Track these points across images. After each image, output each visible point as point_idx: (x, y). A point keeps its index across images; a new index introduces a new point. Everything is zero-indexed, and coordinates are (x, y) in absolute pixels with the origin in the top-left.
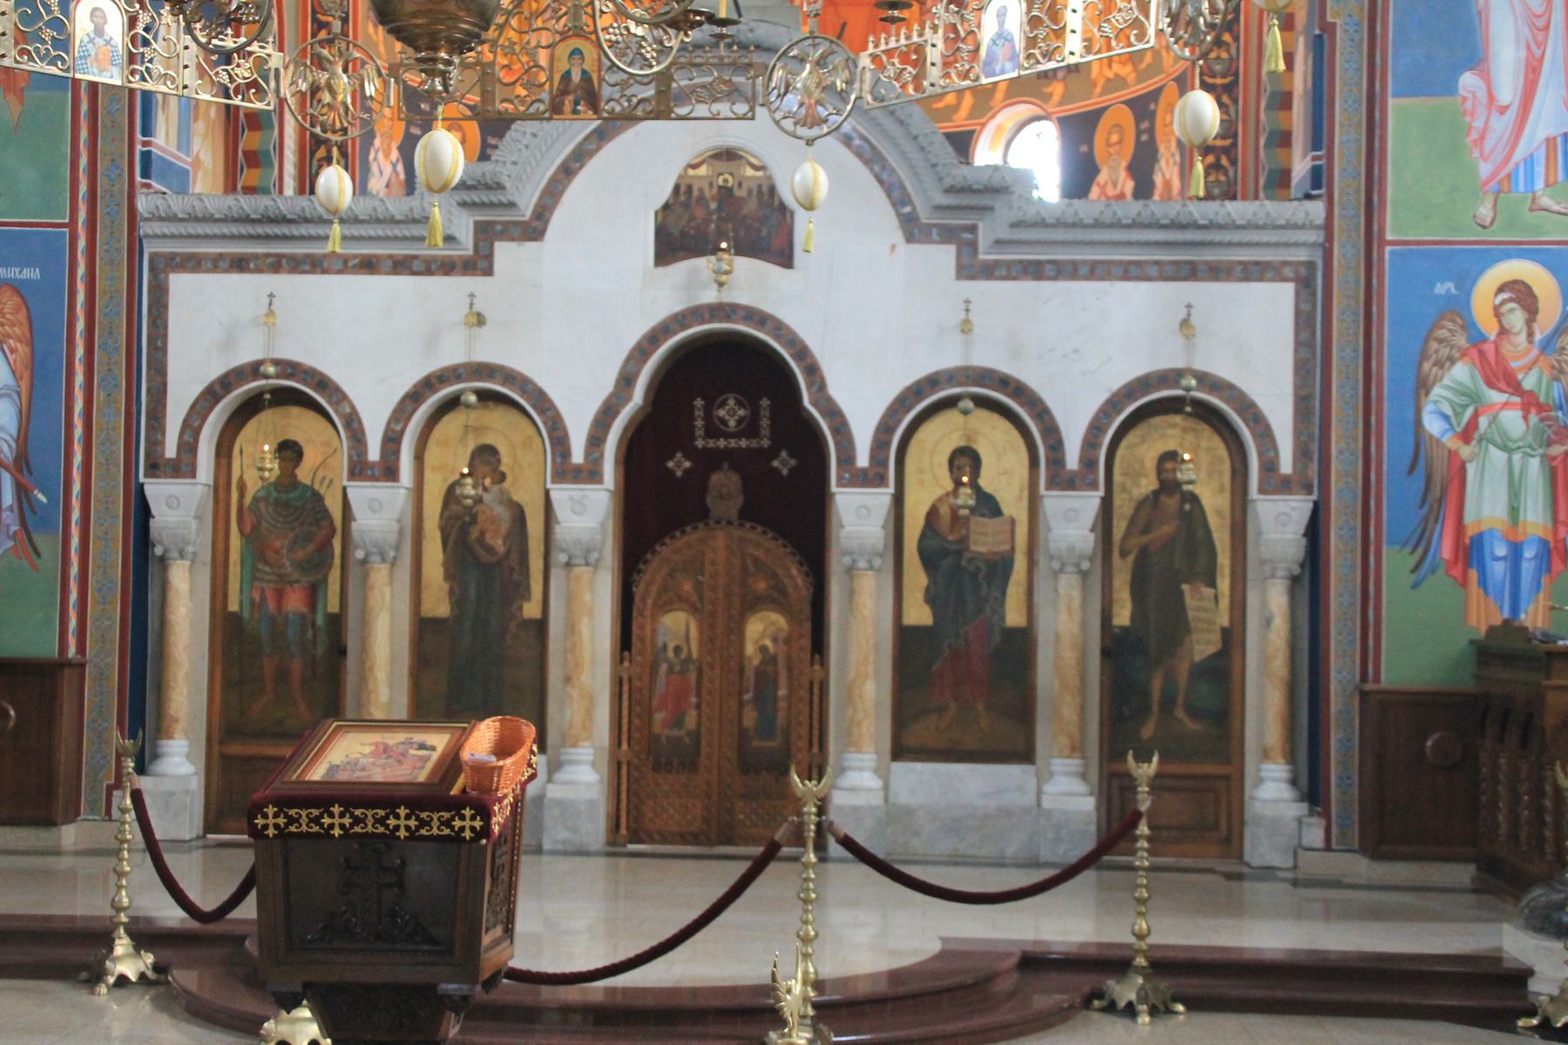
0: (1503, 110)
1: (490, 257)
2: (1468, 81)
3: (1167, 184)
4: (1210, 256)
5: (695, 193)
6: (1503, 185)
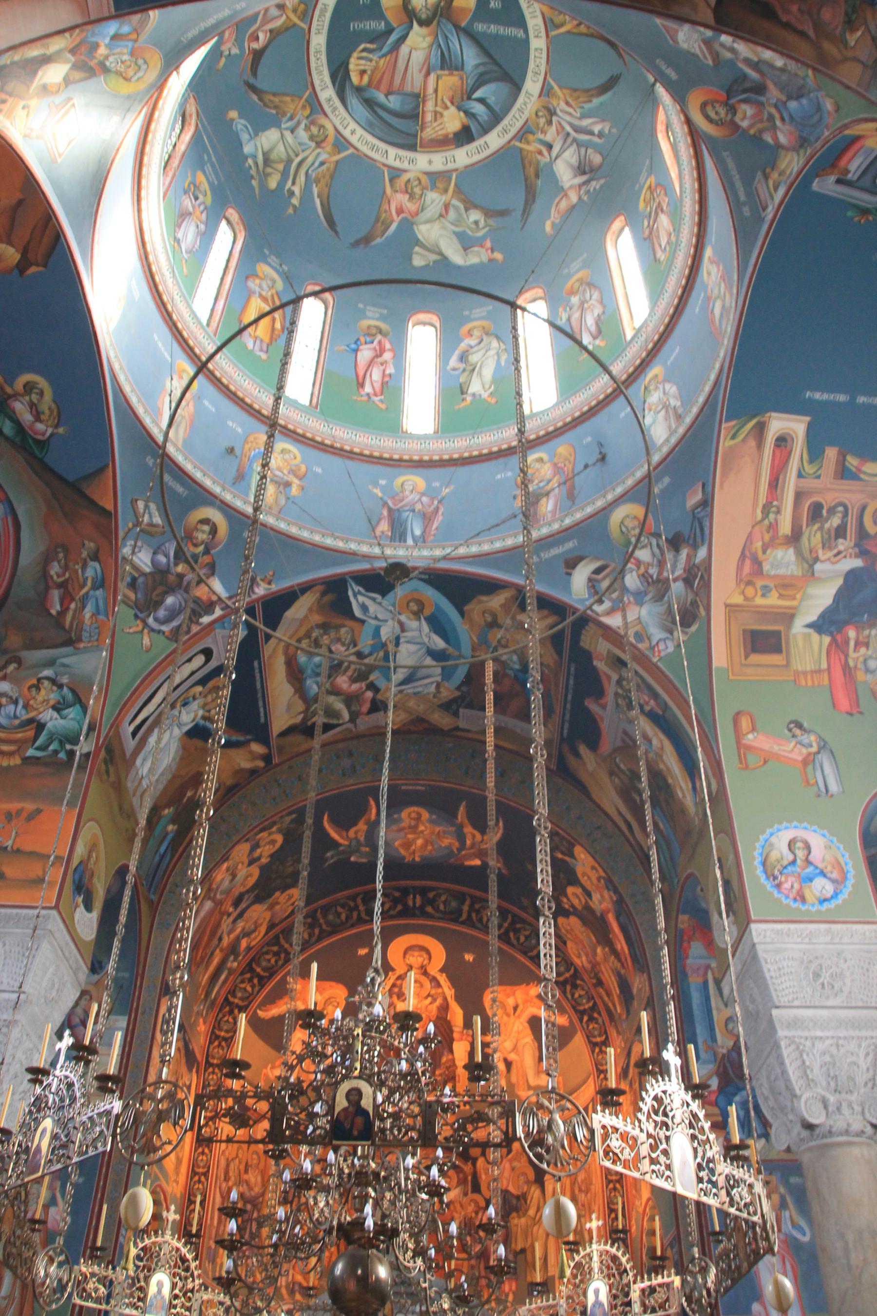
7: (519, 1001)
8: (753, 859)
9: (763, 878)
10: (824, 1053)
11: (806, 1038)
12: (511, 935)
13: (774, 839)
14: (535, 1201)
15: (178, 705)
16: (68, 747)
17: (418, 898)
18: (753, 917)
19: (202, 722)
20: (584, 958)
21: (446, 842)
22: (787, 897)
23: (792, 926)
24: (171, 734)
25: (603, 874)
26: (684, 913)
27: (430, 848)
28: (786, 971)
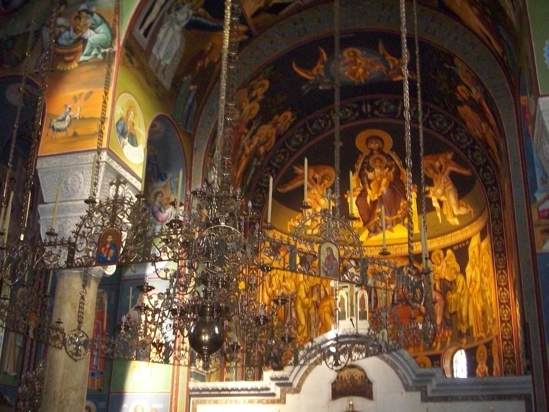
1: (285, 398)
5: (343, 378)
7: (443, 164)
12: (431, 123)
14: (461, 284)
15: (173, 10)
16: (103, 51)
17: (369, 106)
19: (194, 18)
20: (477, 132)
21: (378, 67)
27: (368, 73)
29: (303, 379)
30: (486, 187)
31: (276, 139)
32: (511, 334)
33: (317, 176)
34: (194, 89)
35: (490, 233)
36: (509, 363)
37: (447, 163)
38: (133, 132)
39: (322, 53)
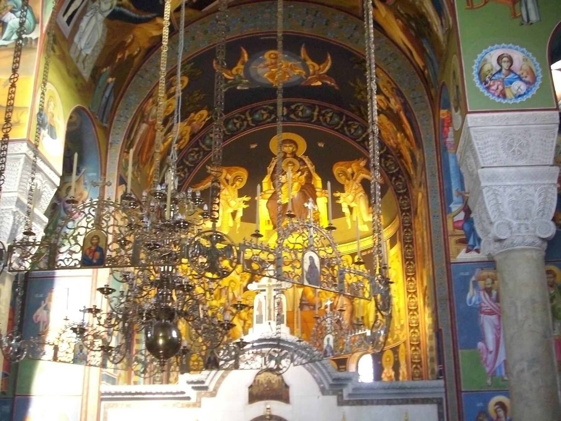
0: (491, 352)
2: (480, 344)
3: (403, 373)
4: (412, 397)
5: (260, 382)
6: (493, 374)
7: (355, 170)
8: (472, 70)
9: (478, 84)
10: (511, 195)
11: (500, 186)
12: (345, 128)
13: (487, 57)
17: (285, 109)
18: (469, 110)
19: (118, 8)
20: (392, 141)
22: (493, 95)
23: (495, 114)
24: (97, 19)
25: (394, 86)
26: (444, 108)
27: (287, 76)
28: (489, 143)
29: (219, 383)
30: (399, 195)
31: (190, 136)
32: (418, 340)
33: (229, 177)
34: (112, 82)
35: (400, 240)
36: (416, 368)
37: (359, 170)
38: (52, 124)
39: (243, 54)
